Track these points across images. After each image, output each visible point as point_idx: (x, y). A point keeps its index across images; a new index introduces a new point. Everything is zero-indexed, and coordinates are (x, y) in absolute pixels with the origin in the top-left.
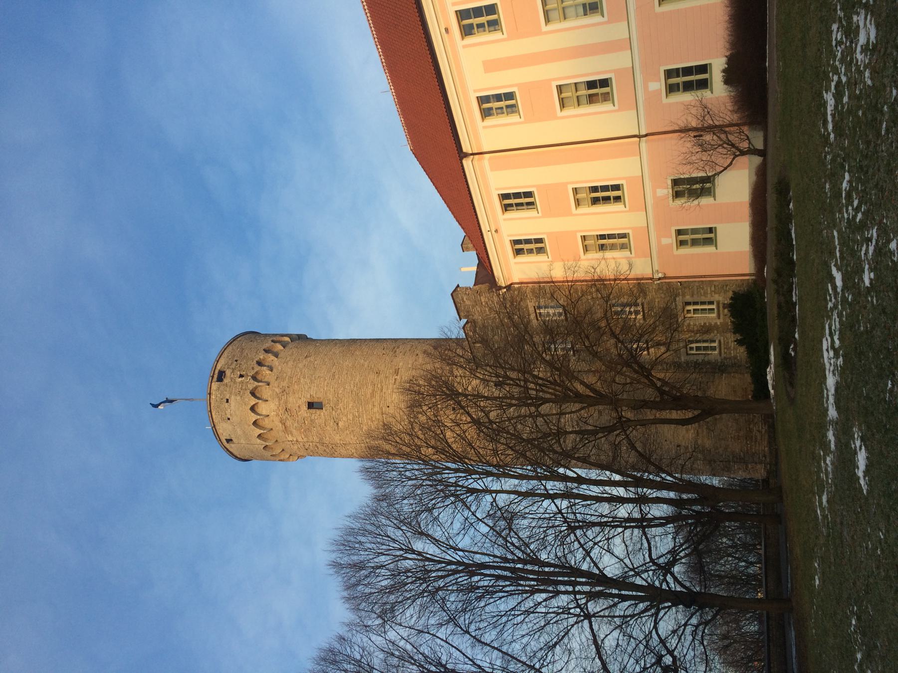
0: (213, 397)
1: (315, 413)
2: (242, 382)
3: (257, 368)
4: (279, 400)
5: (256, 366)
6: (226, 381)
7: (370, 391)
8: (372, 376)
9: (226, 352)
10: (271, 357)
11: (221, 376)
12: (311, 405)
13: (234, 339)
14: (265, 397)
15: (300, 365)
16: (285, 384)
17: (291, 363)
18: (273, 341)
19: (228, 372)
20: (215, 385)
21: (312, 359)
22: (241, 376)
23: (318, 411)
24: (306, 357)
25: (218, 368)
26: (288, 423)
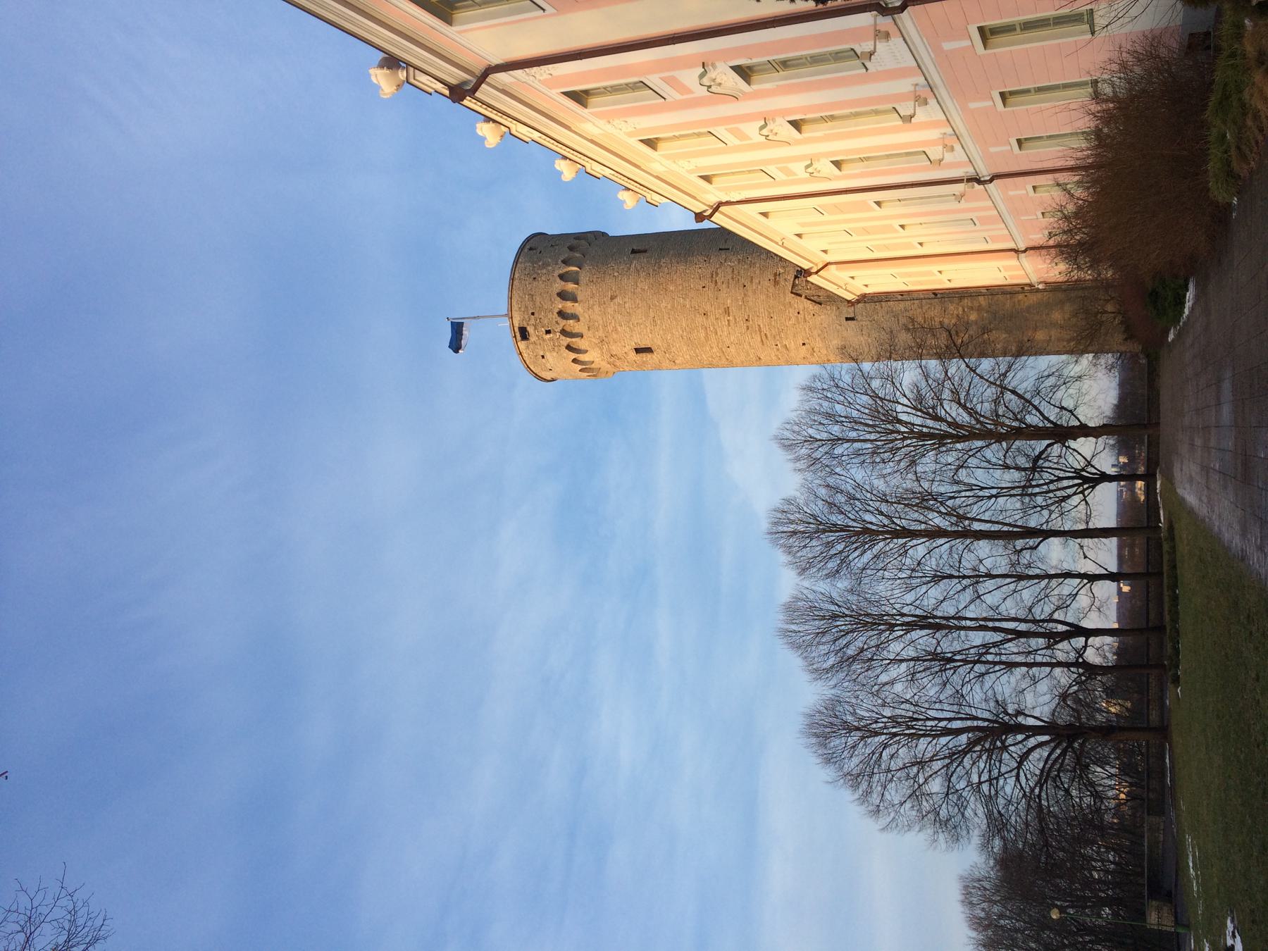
0: (525, 355)
1: (645, 357)
2: (551, 339)
3: (563, 322)
4: (601, 349)
5: (559, 319)
6: (533, 338)
7: (702, 335)
8: (700, 319)
9: (514, 303)
10: (569, 304)
11: (524, 334)
12: (638, 351)
13: (512, 279)
14: (583, 347)
15: (610, 310)
16: (601, 333)
17: (596, 308)
18: (562, 277)
19: (530, 329)
20: (522, 345)
21: (618, 300)
22: (548, 332)
23: (649, 355)
24: (612, 298)
25: (517, 325)
26: (618, 363)
